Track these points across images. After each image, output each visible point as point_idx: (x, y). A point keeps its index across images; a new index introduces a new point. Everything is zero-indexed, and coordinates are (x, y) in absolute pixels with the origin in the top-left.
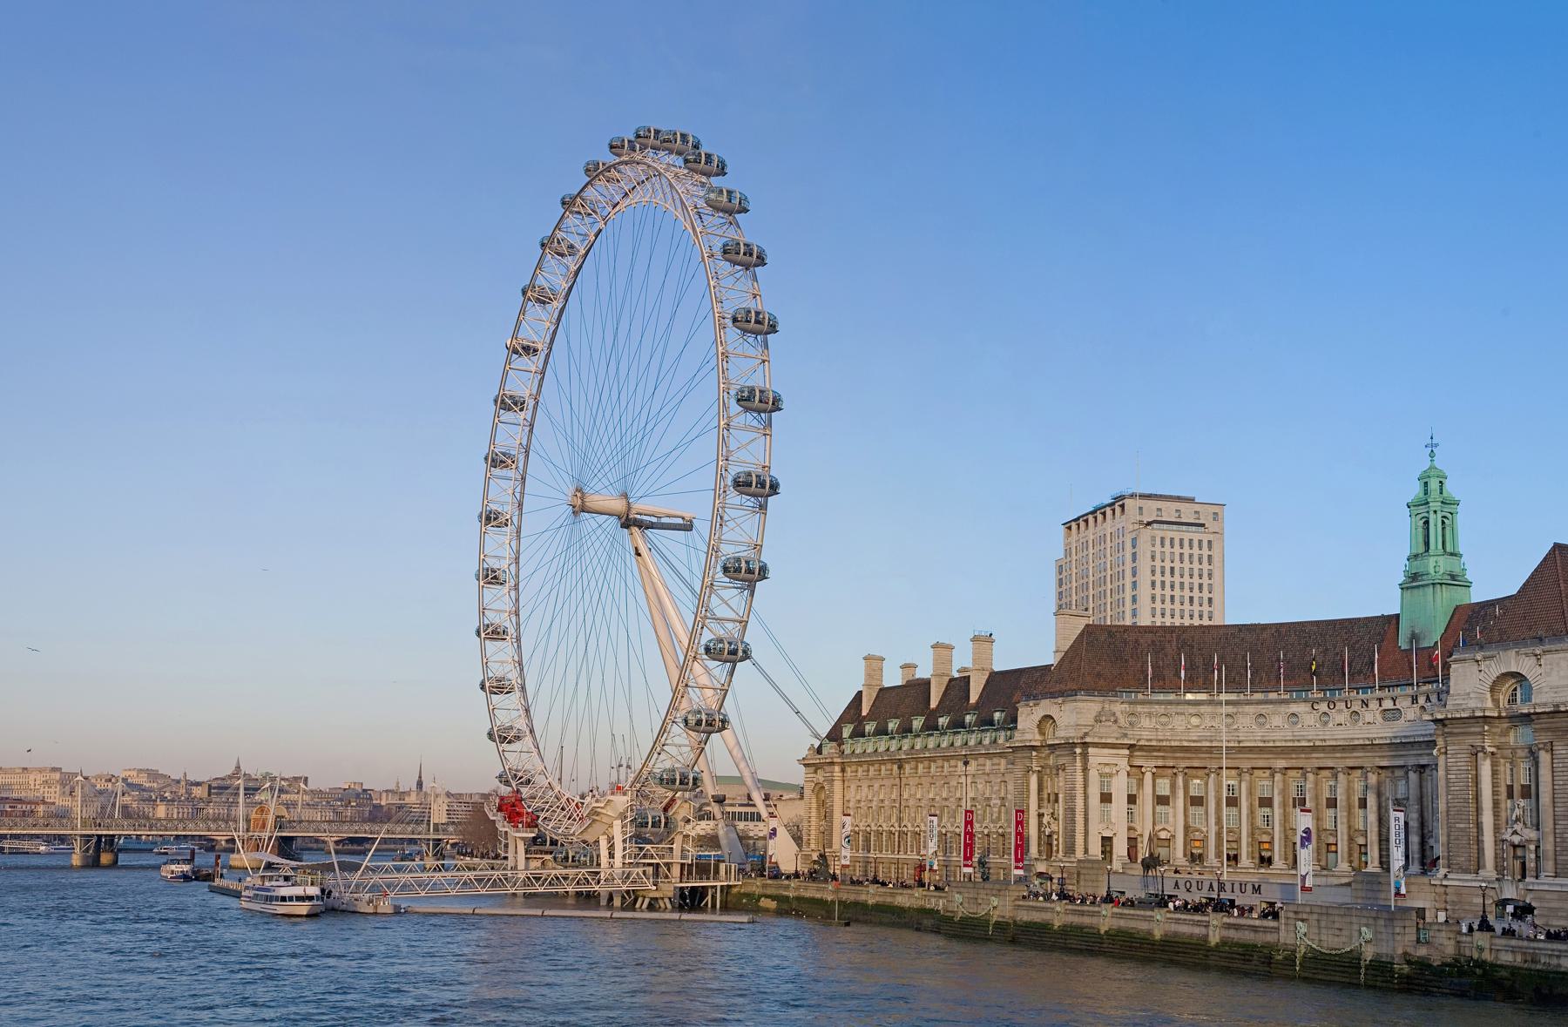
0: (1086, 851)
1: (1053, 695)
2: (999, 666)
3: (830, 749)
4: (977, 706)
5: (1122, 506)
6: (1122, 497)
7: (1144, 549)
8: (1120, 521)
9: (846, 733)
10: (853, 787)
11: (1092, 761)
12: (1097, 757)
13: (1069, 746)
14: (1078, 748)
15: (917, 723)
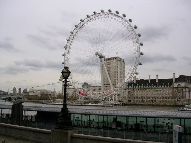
0: (186, 98)
1: (180, 82)
2: (151, 79)
3: (130, 87)
4: (158, 83)
5: (115, 59)
6: (116, 57)
7: (119, 63)
8: (115, 60)
9: (133, 85)
10: (136, 92)
11: (186, 89)
12: (187, 89)
13: (183, 87)
14: (185, 88)
15: (148, 84)
